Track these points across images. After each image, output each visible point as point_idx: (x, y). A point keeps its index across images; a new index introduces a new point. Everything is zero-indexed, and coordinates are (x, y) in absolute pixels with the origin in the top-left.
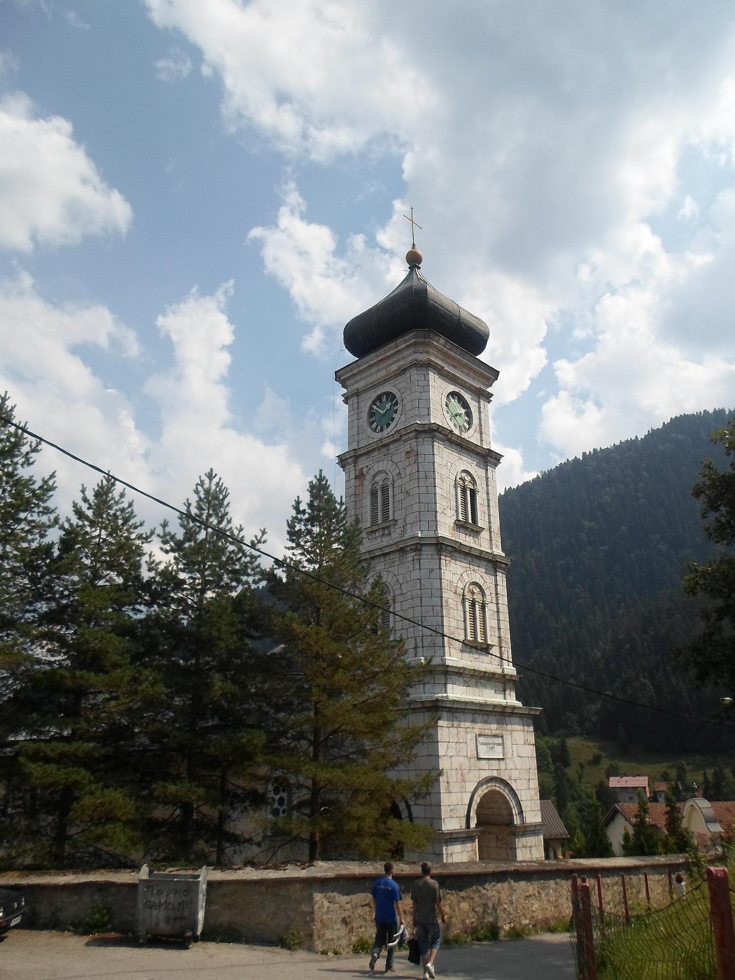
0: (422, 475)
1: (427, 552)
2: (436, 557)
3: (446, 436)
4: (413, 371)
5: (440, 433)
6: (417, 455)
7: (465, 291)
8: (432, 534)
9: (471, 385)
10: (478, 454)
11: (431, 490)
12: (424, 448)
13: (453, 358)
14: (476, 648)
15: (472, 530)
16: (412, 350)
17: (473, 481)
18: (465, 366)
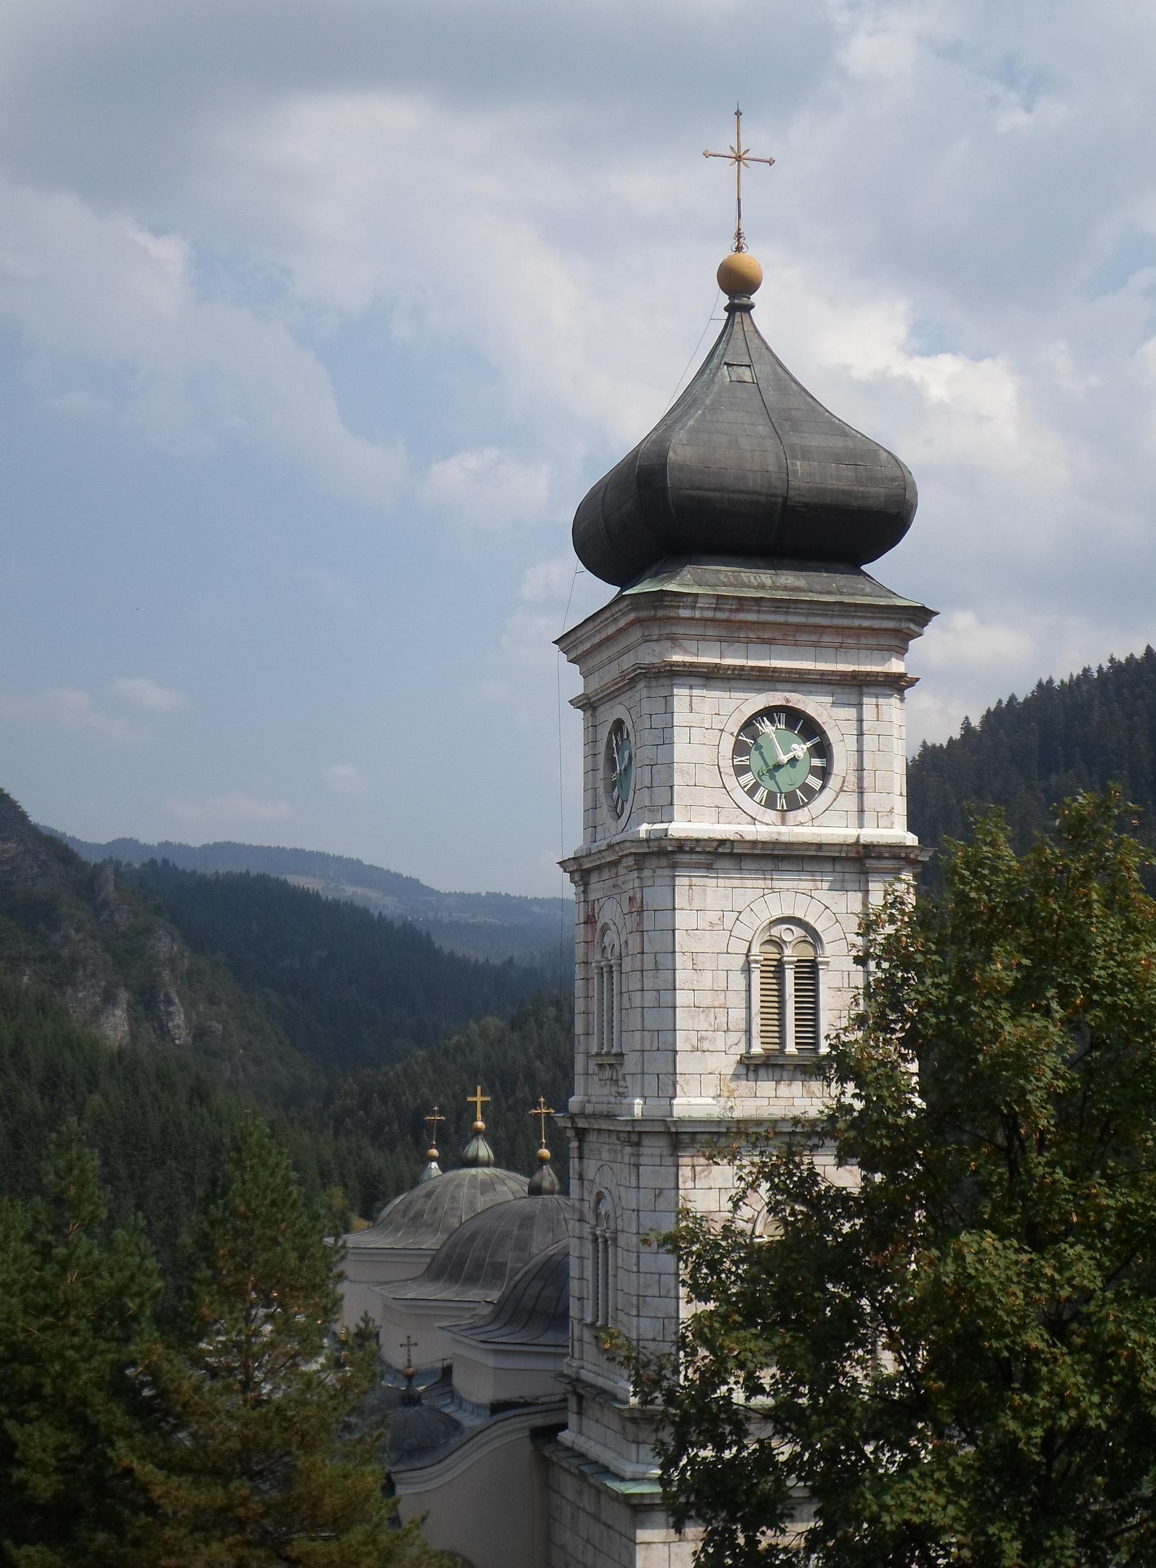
0: (649, 962)
1: (654, 1149)
2: (668, 1161)
4: (641, 689)
5: (692, 851)
6: (641, 912)
7: (859, 358)
8: (657, 1109)
10: (834, 860)
11: (665, 997)
12: (654, 897)
16: (636, 635)
17: (813, 936)
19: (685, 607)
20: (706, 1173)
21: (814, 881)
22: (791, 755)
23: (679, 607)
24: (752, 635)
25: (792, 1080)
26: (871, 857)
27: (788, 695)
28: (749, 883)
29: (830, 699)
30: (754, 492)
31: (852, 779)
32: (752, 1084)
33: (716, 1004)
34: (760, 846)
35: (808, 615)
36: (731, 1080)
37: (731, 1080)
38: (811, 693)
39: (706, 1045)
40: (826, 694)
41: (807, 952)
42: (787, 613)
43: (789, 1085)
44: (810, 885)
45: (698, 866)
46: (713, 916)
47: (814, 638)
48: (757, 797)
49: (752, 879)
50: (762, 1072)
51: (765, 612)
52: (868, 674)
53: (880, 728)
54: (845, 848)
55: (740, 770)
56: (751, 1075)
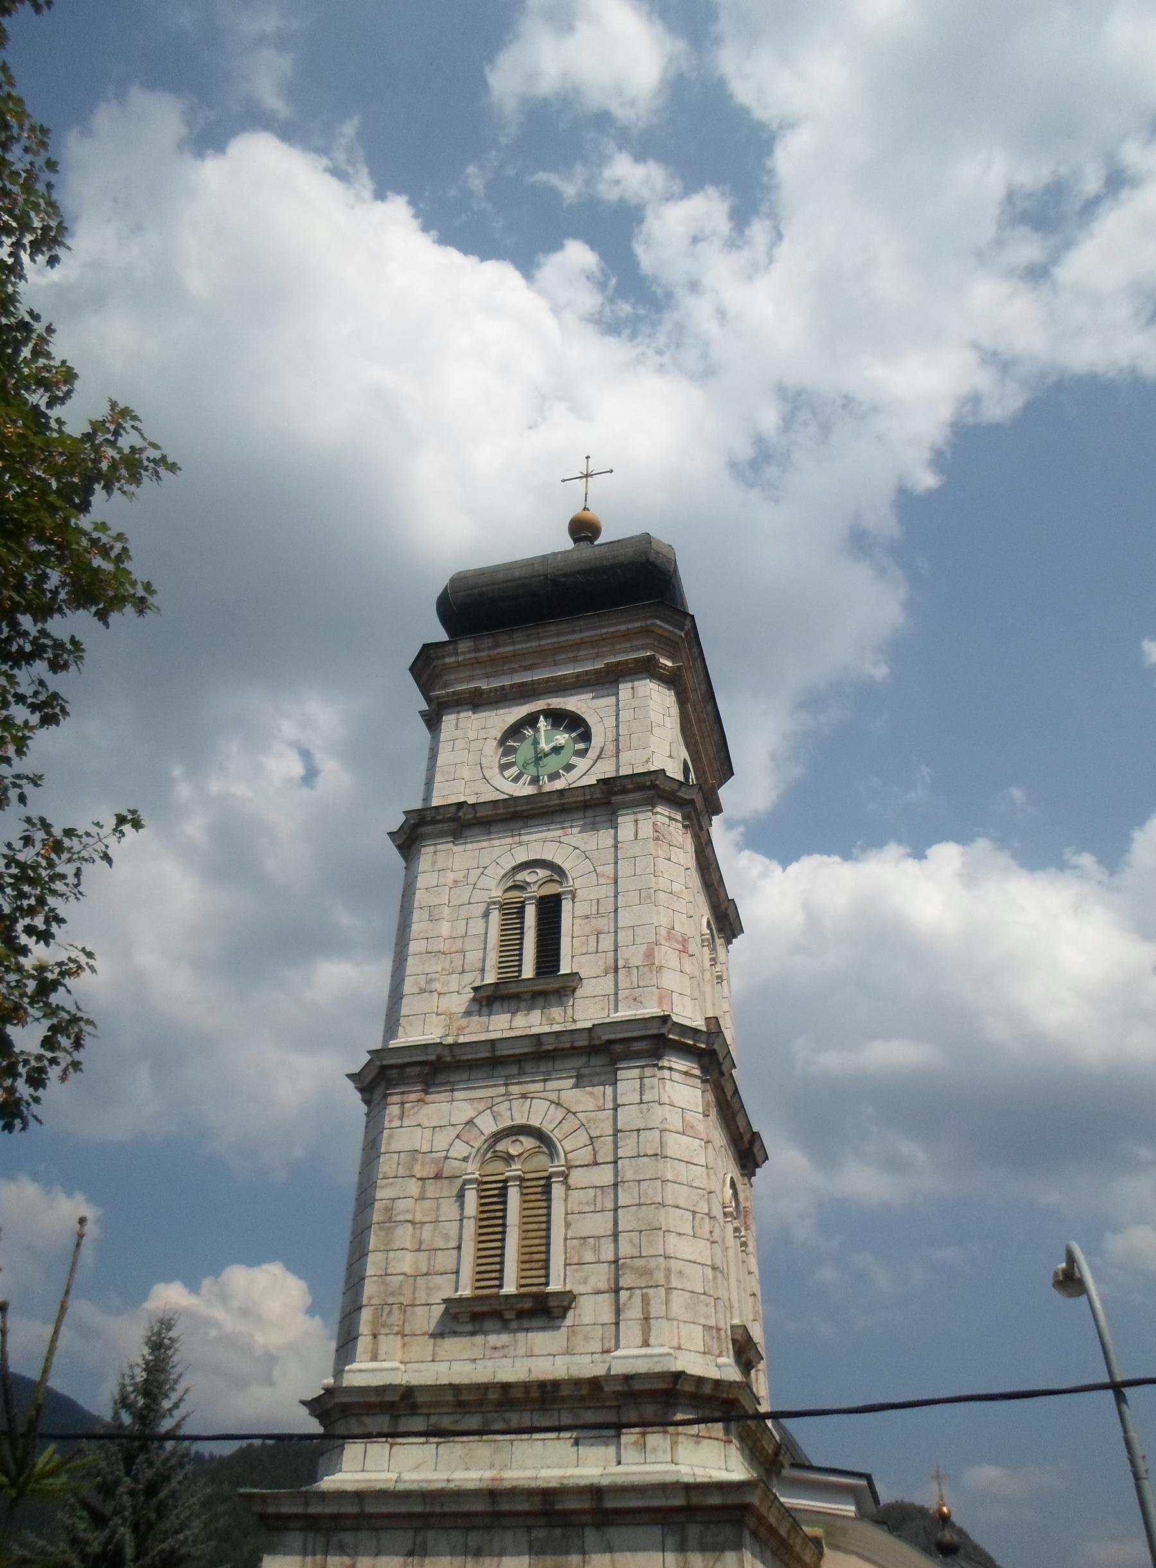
3: (450, 820)
5: (433, 822)
9: (578, 675)
13: (505, 659)
14: (497, 1315)
15: (544, 994)
18: (559, 649)
19: (450, 655)
20: (416, 1109)
21: (563, 828)
22: (553, 744)
23: (444, 657)
24: (514, 666)
25: (530, 1009)
26: (616, 794)
27: (549, 701)
28: (496, 842)
29: (590, 695)
30: (519, 579)
31: (610, 748)
32: (484, 1019)
33: (453, 950)
34: (501, 805)
35: (558, 635)
36: (462, 1017)
37: (462, 1017)
38: (571, 695)
39: (436, 986)
40: (587, 692)
41: (550, 889)
42: (539, 639)
43: (526, 1015)
44: (560, 832)
45: (442, 834)
46: (460, 876)
47: (572, 655)
48: (507, 773)
49: (499, 838)
50: (496, 1006)
51: (519, 643)
52: (618, 664)
53: (635, 703)
54: (587, 791)
55: (504, 767)
56: (485, 1010)
